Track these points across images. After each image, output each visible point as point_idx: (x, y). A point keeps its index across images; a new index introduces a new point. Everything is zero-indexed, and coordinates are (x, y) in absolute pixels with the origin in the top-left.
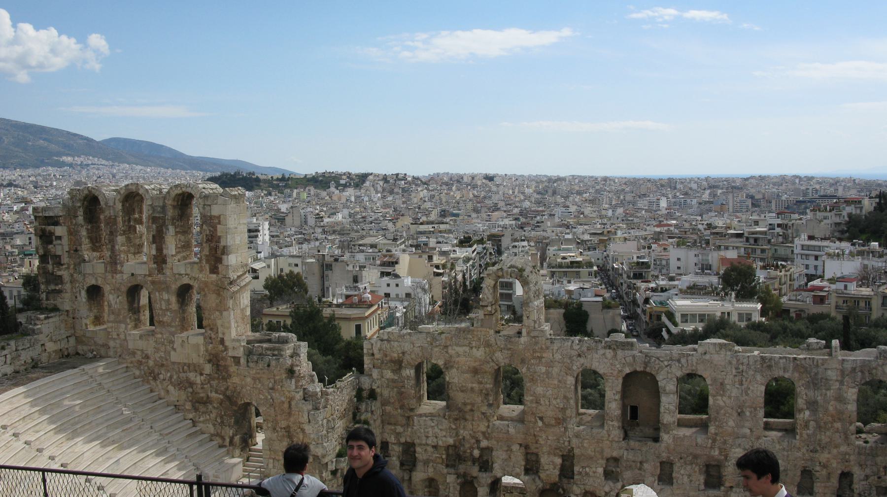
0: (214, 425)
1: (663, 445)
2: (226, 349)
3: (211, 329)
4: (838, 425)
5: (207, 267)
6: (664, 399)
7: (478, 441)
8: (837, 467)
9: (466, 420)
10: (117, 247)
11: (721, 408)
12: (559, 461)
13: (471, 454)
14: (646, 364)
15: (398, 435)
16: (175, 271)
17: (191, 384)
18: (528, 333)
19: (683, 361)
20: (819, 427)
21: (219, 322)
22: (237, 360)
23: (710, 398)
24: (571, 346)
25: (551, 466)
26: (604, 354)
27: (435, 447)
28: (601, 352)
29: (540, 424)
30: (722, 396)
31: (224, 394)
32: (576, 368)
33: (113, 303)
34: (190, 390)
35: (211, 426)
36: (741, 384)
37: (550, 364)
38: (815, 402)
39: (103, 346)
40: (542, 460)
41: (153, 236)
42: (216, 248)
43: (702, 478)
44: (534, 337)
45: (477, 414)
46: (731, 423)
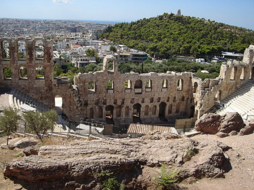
0: (48, 103)
2: (52, 82)
3: (47, 78)
4: (174, 88)
5: (47, 61)
6: (143, 85)
7: (103, 98)
8: (174, 96)
9: (100, 93)
10: (15, 56)
11: (154, 86)
12: (121, 100)
13: (102, 101)
15: (84, 99)
16: (36, 62)
17: (41, 93)
20: (171, 88)
21: (50, 75)
22: (55, 85)
27: (93, 101)
31: (51, 94)
33: (13, 72)
34: (40, 94)
35: (47, 103)
37: (120, 79)
38: (171, 84)
39: (10, 85)
41: (29, 53)
42: (50, 56)
45: (103, 92)
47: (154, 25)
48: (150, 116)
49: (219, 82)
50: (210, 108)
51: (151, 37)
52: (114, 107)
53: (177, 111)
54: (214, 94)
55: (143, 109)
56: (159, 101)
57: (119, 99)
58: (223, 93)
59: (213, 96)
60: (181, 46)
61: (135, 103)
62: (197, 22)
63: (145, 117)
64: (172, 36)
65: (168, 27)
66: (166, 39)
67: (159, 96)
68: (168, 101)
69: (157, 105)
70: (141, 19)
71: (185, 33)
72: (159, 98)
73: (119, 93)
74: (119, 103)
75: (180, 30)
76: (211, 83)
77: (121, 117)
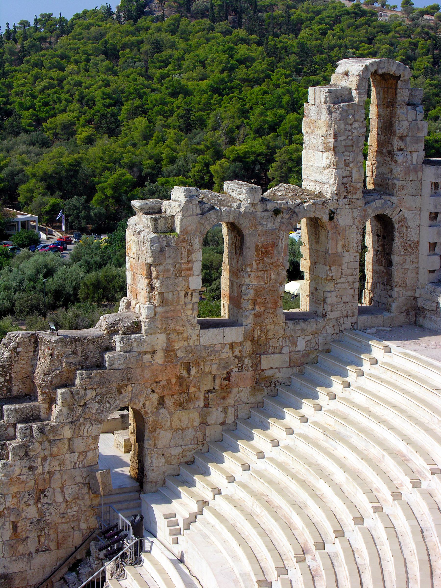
47: (89, 48)
49: (110, 348)
50: (63, 553)
51: (62, 118)
54: (80, 445)
58: (157, 426)
59: (70, 459)
60: (218, 155)
62: (338, 19)
64: (179, 101)
65: (166, 53)
66: (141, 122)
70: (24, 23)
71: (258, 82)
75: (232, 69)
76: (43, 364)
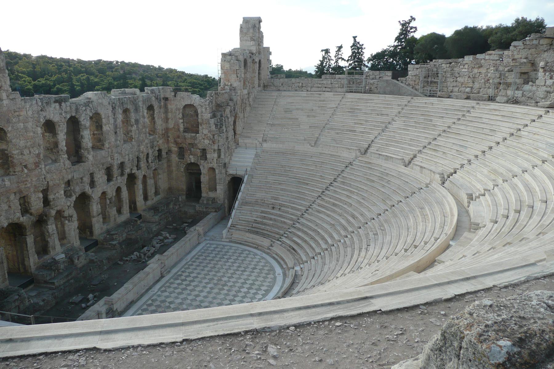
1: (90, 163)
8: (145, 151)
12: (41, 195)
14: (77, 110)
18: (8, 96)
19: (91, 105)
23: (104, 126)
24: (37, 103)
25: (36, 204)
26: (55, 108)
28: (53, 105)
29: (26, 171)
30: (108, 124)
32: (42, 121)
36: (114, 116)
40: (32, 199)
43: (106, 177)
44: (12, 99)
46: (113, 140)
48: (115, 220)
52: (27, 227)
53: (156, 193)
55: (95, 208)
56: (122, 174)
57: (35, 192)
61: (78, 190)
63: (105, 227)
67: (122, 160)
68: (138, 168)
69: (122, 187)
72: (122, 165)
73: (33, 170)
74: (36, 204)
77: (52, 253)
